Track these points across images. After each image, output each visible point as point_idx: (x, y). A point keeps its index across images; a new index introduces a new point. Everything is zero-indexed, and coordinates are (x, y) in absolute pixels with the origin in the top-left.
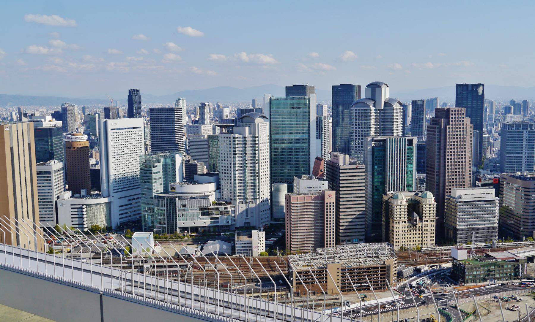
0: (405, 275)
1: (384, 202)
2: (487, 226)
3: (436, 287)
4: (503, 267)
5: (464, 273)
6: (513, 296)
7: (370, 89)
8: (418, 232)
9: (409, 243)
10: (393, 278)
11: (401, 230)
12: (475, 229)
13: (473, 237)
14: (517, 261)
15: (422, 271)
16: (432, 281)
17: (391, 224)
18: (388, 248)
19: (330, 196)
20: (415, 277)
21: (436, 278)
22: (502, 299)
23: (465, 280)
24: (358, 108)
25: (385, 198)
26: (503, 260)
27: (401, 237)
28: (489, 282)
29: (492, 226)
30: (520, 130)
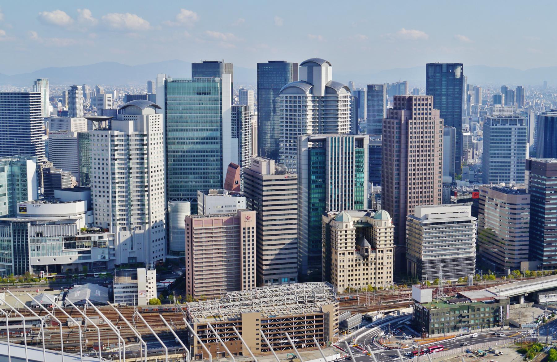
0: (350, 326)
1: (324, 225)
2: (461, 256)
3: (391, 340)
4: (478, 310)
5: (429, 320)
6: (490, 349)
7: (306, 68)
8: (370, 267)
9: (358, 282)
10: (333, 330)
11: (346, 264)
12: (443, 261)
13: (441, 272)
14: (497, 301)
15: (374, 319)
16: (387, 332)
17: (333, 256)
18: (326, 288)
19: (248, 218)
20: (364, 328)
21: (392, 329)
22: (477, 354)
23: (430, 330)
24: (289, 95)
25: (325, 220)
26: (480, 301)
27: (346, 273)
28: (461, 331)
29: (467, 255)
30: (508, 126)
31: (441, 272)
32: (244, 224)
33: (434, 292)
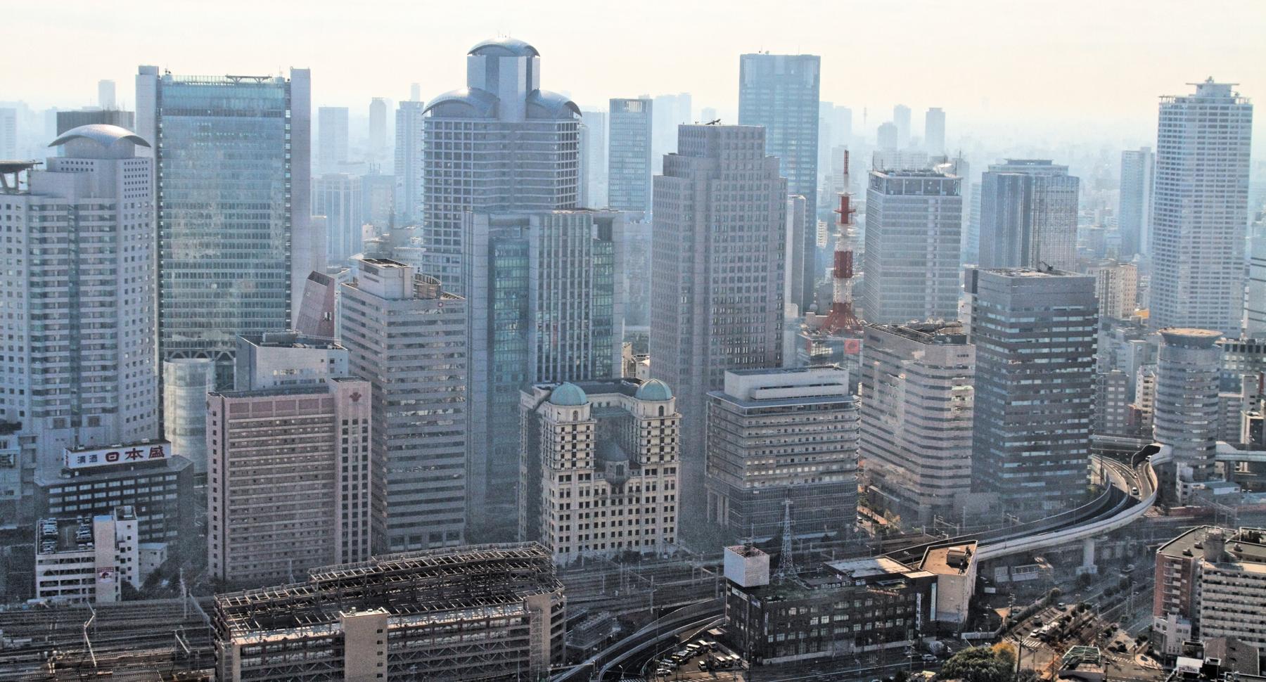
2: (827, 479)
9: (600, 541)
11: (575, 500)
17: (545, 483)
19: (355, 397)
27: (575, 523)
32: (345, 409)
33: (774, 564)
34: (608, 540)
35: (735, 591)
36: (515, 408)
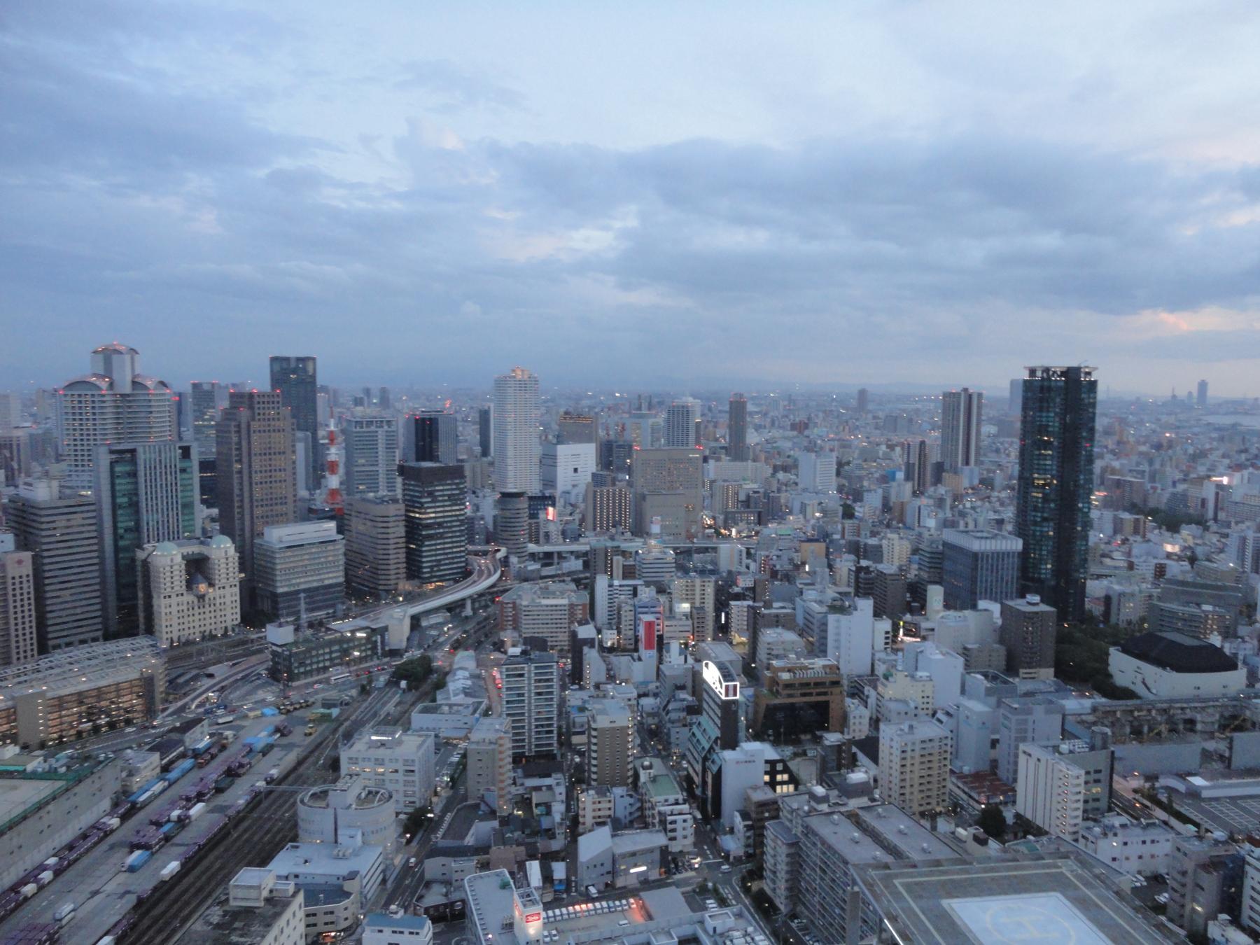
1: (139, 563)
2: (327, 582)
8: (207, 609)
9: (192, 631)
11: (174, 609)
12: (304, 591)
13: (302, 601)
17: (155, 602)
25: (141, 555)
27: (175, 622)
31: (302, 601)
33: (297, 630)
34: (197, 630)
35: (275, 648)
36: (133, 560)
